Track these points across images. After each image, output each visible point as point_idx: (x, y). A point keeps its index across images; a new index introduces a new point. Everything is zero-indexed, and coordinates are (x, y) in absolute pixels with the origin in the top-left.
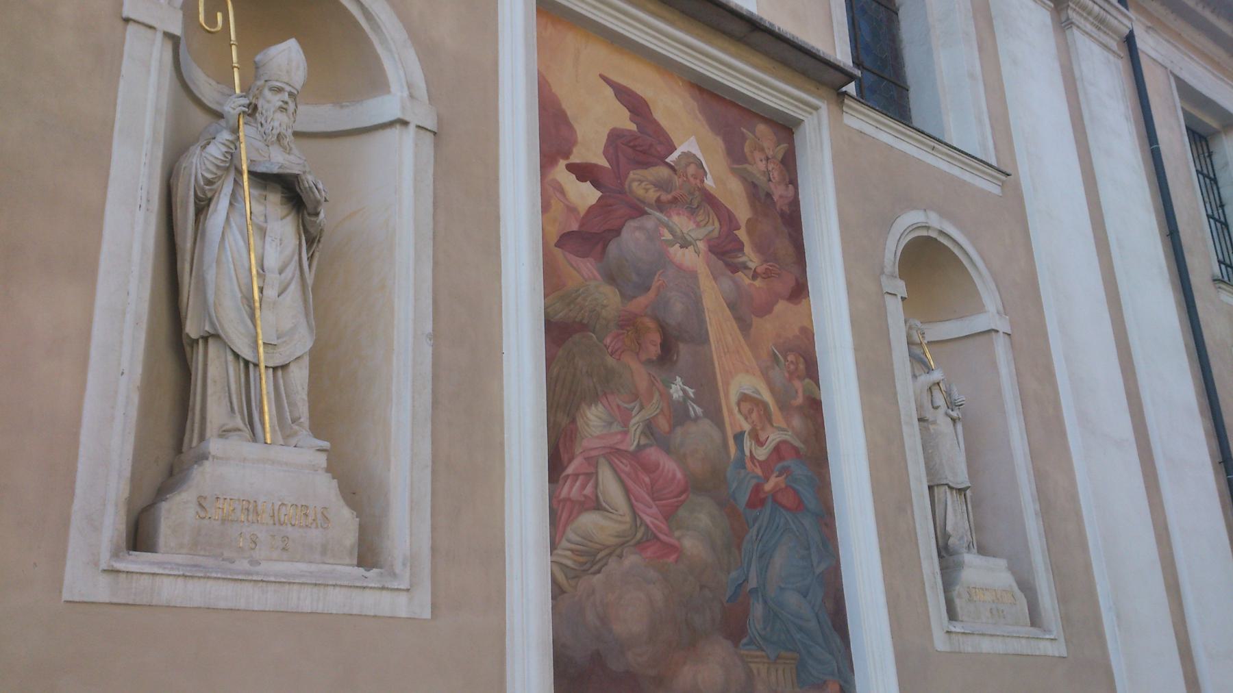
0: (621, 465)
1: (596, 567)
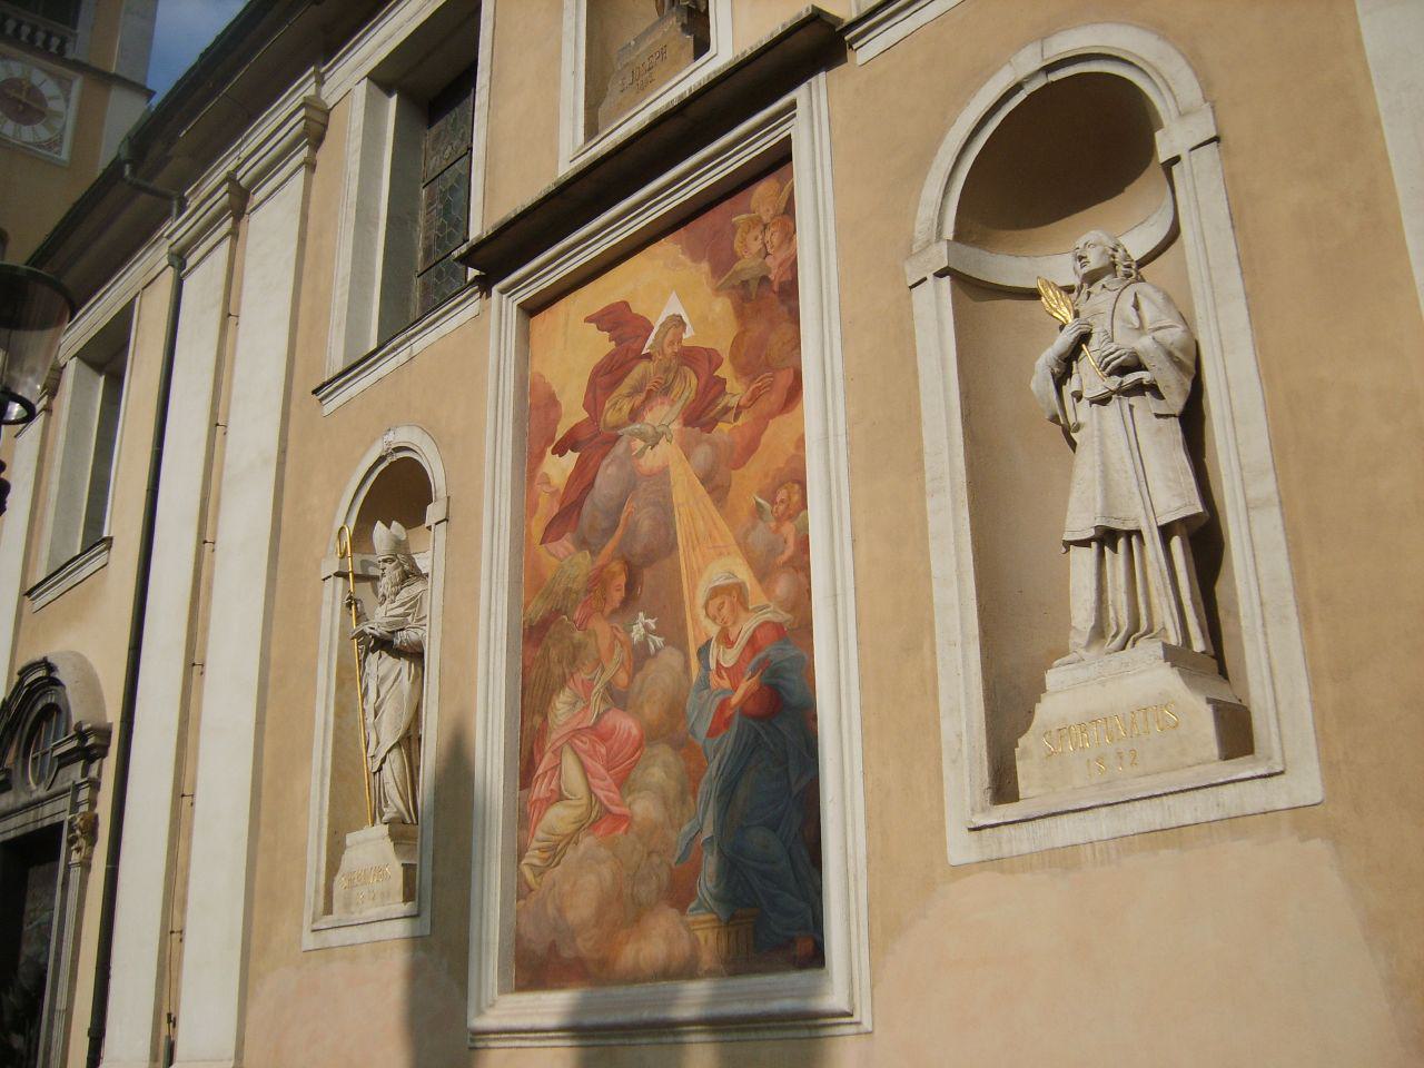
0: (580, 744)
1: (556, 860)
